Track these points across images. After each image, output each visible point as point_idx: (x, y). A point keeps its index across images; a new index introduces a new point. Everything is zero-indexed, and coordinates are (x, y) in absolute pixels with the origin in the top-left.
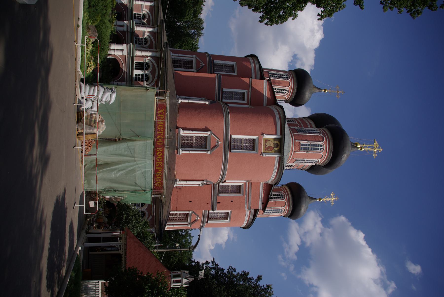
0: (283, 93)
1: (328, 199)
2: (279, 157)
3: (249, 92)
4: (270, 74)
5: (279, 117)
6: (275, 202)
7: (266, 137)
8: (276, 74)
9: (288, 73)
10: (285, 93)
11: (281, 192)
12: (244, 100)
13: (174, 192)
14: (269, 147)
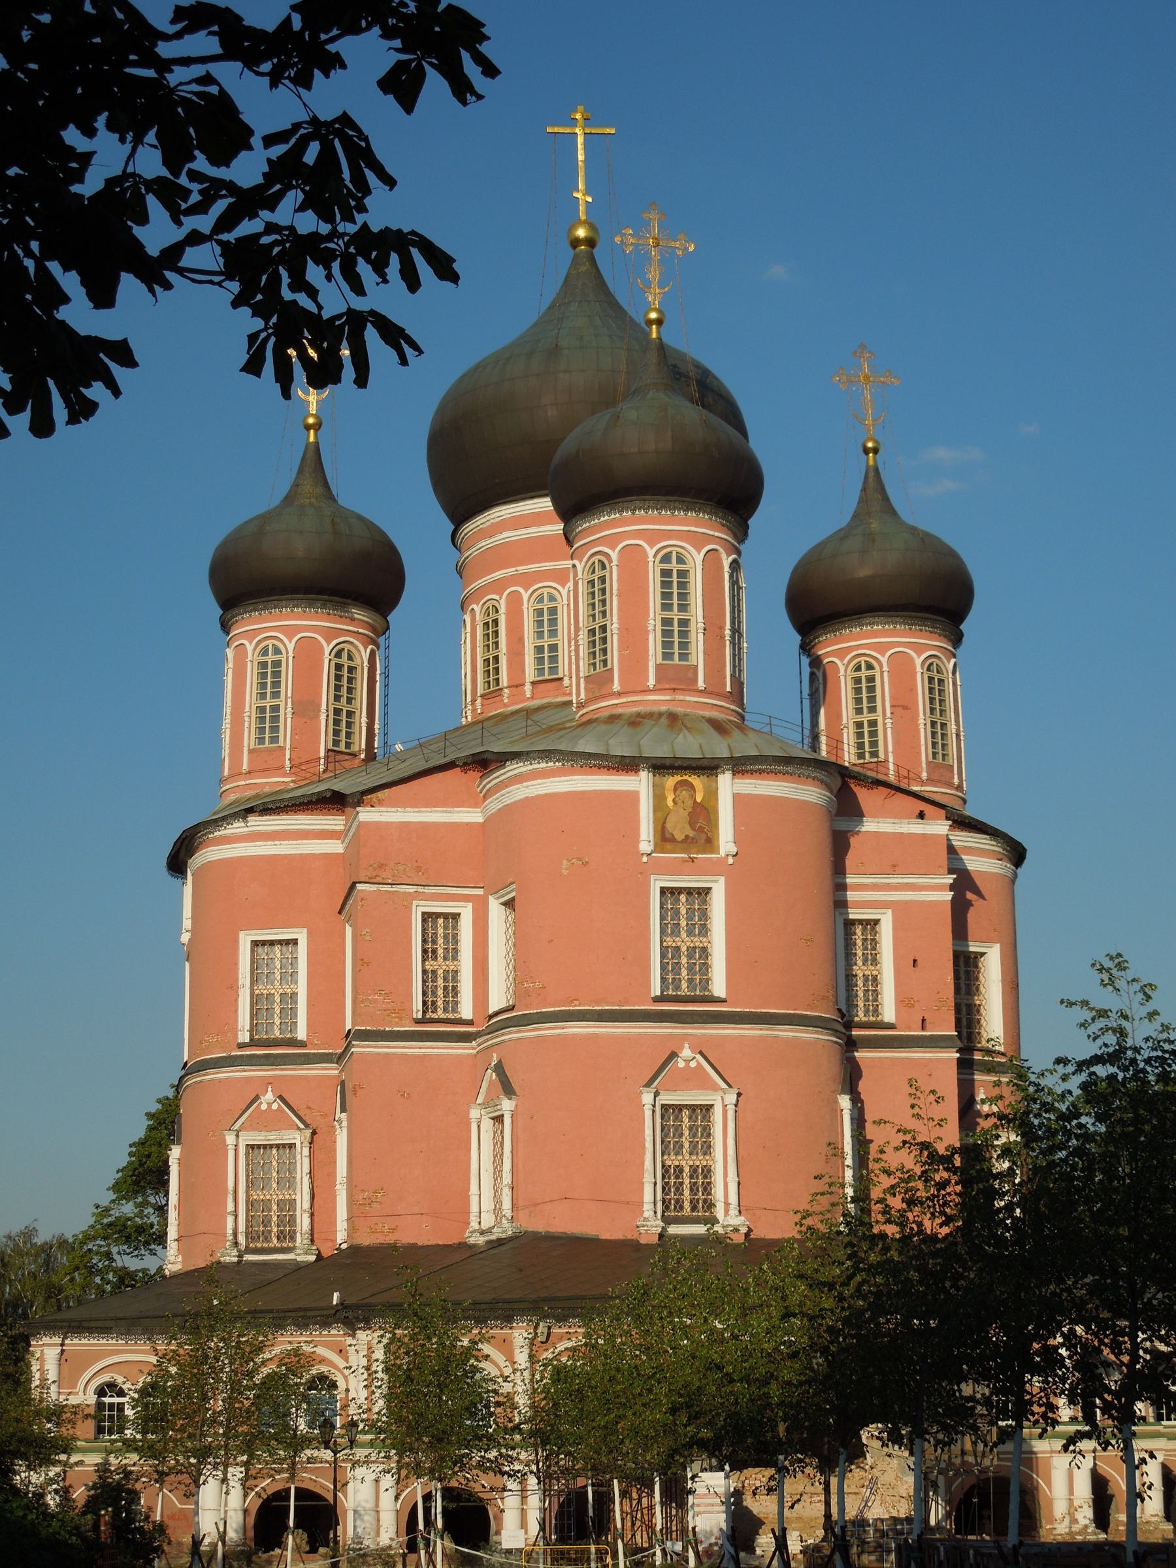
2: (736, 781)
3: (417, 896)
5: (557, 779)
6: (892, 706)
7: (646, 844)
9: (245, 642)
10: (350, 658)
11: (842, 672)
14: (692, 824)
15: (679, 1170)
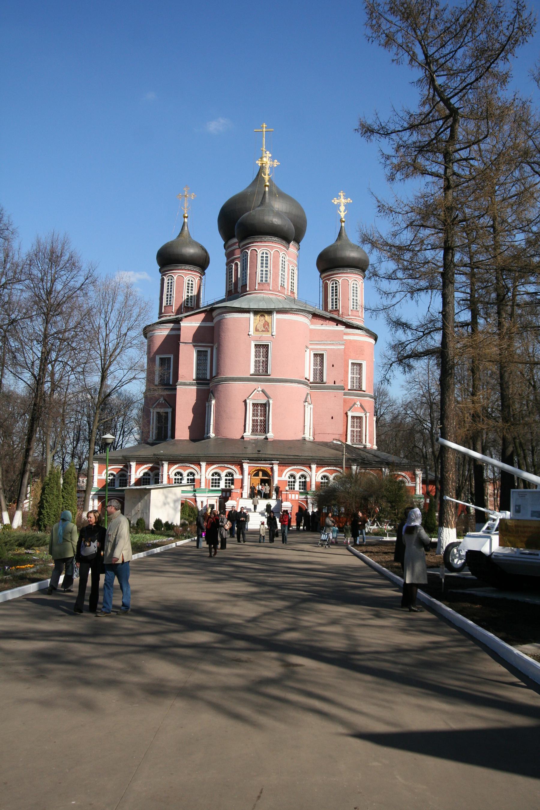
0: (192, 284)
1: (342, 208)
4: (167, 304)
8: (167, 295)
10: (192, 281)
12: (207, 351)
13: (318, 439)
14: (264, 327)
15: (257, 420)
